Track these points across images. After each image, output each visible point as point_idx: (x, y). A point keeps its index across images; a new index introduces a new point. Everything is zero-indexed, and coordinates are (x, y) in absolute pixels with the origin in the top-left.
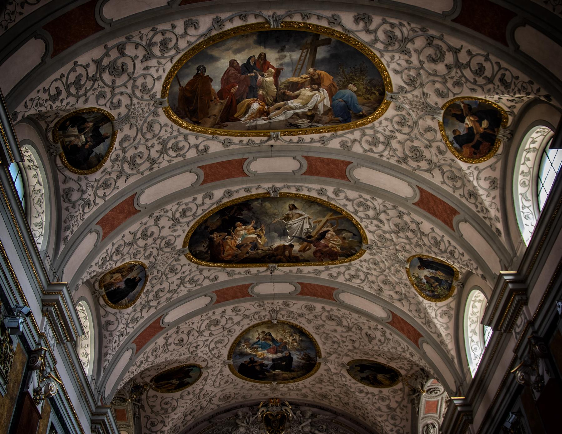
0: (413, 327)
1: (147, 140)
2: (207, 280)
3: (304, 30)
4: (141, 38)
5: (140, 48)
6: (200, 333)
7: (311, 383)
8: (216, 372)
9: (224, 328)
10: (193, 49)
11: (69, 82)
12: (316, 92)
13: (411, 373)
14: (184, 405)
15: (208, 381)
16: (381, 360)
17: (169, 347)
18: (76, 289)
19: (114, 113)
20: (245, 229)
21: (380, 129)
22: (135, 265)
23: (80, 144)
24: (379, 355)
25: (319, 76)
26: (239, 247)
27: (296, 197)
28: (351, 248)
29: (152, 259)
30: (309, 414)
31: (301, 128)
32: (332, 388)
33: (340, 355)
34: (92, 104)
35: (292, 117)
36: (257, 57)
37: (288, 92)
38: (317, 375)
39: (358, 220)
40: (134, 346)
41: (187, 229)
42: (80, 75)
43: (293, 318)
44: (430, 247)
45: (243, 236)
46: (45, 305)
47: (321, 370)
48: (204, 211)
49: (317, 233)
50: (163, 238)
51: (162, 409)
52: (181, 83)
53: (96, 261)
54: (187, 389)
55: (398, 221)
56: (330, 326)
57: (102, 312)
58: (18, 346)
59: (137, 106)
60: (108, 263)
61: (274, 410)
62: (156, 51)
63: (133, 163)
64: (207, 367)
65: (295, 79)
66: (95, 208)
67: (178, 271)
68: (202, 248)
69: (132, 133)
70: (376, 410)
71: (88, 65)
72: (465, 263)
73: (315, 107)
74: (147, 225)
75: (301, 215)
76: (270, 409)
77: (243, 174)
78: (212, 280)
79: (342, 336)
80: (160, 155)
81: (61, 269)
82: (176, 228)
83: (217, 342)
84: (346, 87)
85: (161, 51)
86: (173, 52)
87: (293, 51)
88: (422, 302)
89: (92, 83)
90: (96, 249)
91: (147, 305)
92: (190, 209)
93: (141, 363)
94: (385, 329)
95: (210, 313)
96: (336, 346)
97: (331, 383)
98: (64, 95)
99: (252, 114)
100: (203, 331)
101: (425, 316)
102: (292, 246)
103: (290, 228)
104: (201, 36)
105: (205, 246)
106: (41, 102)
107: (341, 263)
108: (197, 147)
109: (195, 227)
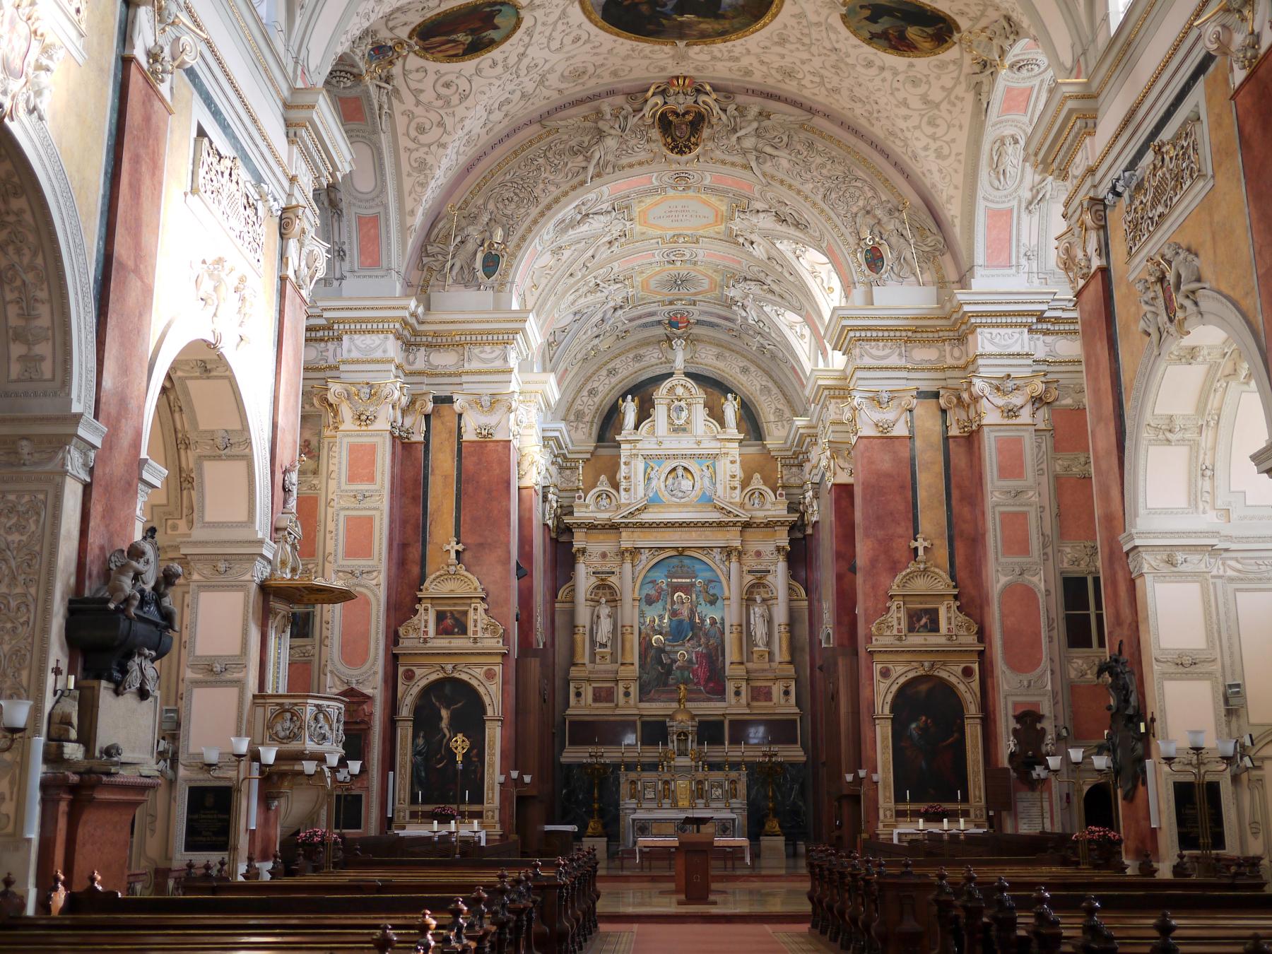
7: (762, 44)
14: (486, 89)
15: (536, 37)
30: (754, 111)
32: (805, 56)
51: (439, 97)
54: (489, 55)
61: (681, 103)
70: (896, 106)
76: (671, 100)
97: (804, 45)
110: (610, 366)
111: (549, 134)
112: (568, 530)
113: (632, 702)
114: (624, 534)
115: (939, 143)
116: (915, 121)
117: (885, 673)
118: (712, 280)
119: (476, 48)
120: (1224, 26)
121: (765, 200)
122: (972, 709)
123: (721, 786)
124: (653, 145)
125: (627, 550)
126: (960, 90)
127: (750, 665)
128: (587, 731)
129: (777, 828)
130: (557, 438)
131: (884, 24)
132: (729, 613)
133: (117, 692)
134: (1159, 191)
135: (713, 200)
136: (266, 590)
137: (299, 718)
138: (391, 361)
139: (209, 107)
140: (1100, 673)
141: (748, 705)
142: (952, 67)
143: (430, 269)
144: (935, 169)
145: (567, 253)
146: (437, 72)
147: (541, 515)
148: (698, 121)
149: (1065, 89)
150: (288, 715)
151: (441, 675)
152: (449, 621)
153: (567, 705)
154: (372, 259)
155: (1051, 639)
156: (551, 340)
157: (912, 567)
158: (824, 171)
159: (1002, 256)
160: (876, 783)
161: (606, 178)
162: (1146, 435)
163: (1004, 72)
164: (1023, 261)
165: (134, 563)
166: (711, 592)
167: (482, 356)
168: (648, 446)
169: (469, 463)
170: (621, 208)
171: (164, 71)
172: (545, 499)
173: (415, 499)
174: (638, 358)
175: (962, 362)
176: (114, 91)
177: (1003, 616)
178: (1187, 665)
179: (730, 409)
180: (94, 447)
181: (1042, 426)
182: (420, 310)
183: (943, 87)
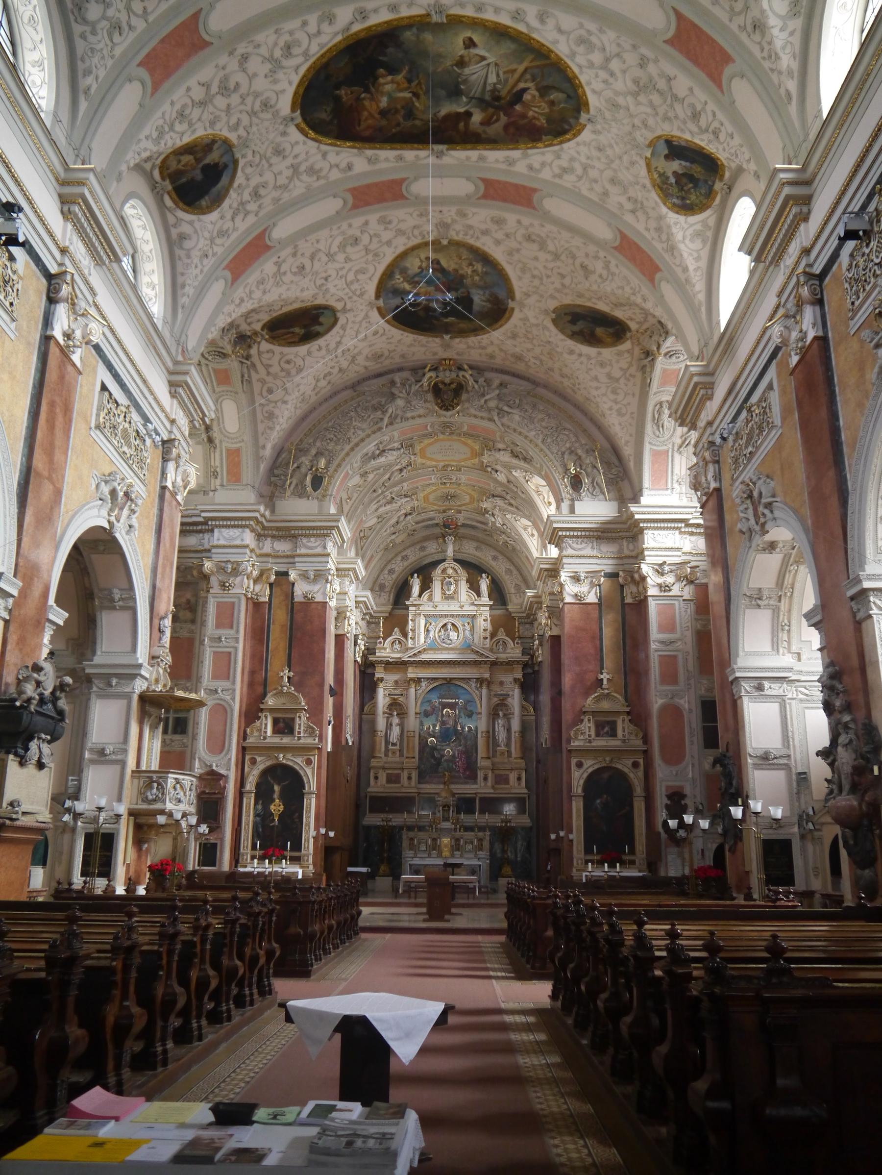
0: (649, 257)
2: (335, 170)
6: (331, 256)
8: (359, 319)
9: (367, 251)
13: (644, 327)
15: (348, 331)
18: (119, 178)
20: (392, 82)
22: (214, 142)
24: (599, 299)
26: (383, 113)
28: (564, 120)
29: (241, 132)
30: (496, 382)
32: (530, 346)
33: (542, 296)
41: (296, 79)
43: (472, 237)
46: (65, 201)
47: (515, 321)
48: (322, 46)
49: (509, 92)
50: (257, 95)
51: (282, 370)
53: (146, 131)
55: (638, 73)
57: (171, 219)
58: (27, 265)
60: (167, 137)
61: (447, 376)
64: (344, 310)
66: (132, 36)
67: (287, 153)
72: (733, 151)
74: (228, 70)
75: (483, 58)
76: (441, 374)
79: (545, 267)
83: (357, 272)
90: (143, 113)
91: (240, 209)
92: (298, 43)
93: (242, 300)
94: (609, 258)
95: (344, 225)
100: (335, 253)
101: (668, 239)
102: (468, 114)
103: (465, 81)
105: (329, 109)
107: (546, 146)
109: (310, 76)
110: (404, 554)
111: (358, 396)
112: (372, 665)
113: (413, 783)
114: (410, 670)
115: (619, 406)
117: (580, 765)
118: (472, 497)
119: (308, 337)
120: (785, 327)
121: (503, 441)
122: (639, 790)
123: (472, 842)
124: (429, 405)
125: (411, 679)
126: (633, 370)
127: (496, 760)
128: (382, 804)
129: (510, 873)
131: (580, 326)
132: (481, 724)
133: (22, 764)
135: (470, 441)
136: (144, 699)
137: (163, 788)
138: (247, 546)
139: (110, 371)
140: (714, 765)
141: (493, 787)
142: (626, 355)
143: (275, 485)
145: (371, 477)
146: (281, 353)
147: (353, 654)
148: (459, 389)
149: (692, 369)
150: (155, 785)
151: (275, 762)
152: (281, 725)
153: (368, 785)
154: (235, 476)
155: (692, 743)
157: (599, 691)
158: (544, 424)
159: (662, 479)
160: (571, 841)
161: (396, 426)
162: (744, 602)
164: (676, 485)
165: (35, 675)
167: (310, 544)
168: (427, 608)
169: (298, 617)
170: (408, 445)
171: (74, 346)
172: (356, 643)
173: (261, 641)
175: (634, 553)
176: (38, 358)
177: (661, 726)
178: (765, 759)
179: (484, 585)
180: (13, 596)
182: (267, 513)
183: (621, 369)
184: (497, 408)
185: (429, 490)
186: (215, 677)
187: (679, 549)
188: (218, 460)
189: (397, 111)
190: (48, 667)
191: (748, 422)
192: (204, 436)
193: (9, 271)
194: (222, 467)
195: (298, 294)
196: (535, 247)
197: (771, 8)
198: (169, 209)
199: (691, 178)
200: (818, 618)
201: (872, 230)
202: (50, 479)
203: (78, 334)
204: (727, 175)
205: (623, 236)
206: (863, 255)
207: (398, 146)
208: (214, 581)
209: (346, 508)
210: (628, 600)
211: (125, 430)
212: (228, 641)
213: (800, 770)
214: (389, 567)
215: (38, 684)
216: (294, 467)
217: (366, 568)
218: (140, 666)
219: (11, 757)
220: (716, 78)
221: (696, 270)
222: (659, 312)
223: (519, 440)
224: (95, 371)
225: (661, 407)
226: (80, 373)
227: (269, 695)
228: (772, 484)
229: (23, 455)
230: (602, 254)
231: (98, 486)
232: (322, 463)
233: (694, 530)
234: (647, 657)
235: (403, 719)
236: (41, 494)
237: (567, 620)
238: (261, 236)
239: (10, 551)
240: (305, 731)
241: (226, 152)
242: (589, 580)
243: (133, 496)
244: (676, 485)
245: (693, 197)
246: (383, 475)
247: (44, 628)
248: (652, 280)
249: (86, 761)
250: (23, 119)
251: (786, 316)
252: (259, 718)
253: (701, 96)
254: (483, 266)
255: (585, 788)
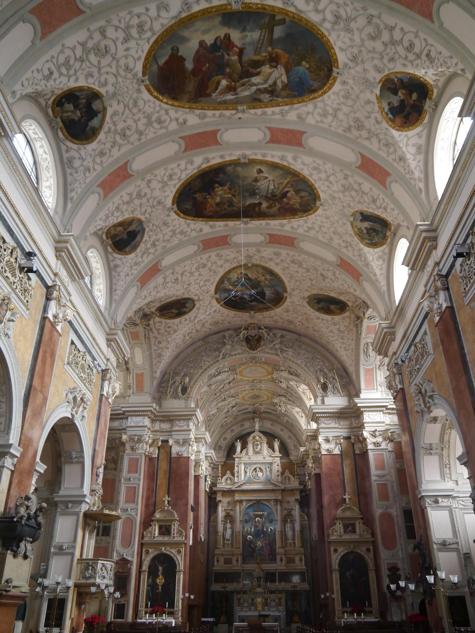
1: (134, 114)
2: (194, 232)
3: (261, 11)
4: (120, 21)
5: (120, 31)
6: (191, 274)
8: (206, 304)
9: (210, 270)
10: (166, 31)
11: (59, 63)
12: (275, 69)
15: (201, 311)
16: (333, 294)
17: (167, 285)
18: (86, 239)
19: (102, 91)
20: (222, 190)
21: (329, 102)
22: (133, 220)
23: (76, 118)
24: (331, 291)
25: (277, 54)
26: (218, 204)
27: (262, 162)
29: (147, 215)
30: (279, 335)
31: (263, 102)
32: (296, 316)
33: (301, 290)
34: (82, 83)
35: (255, 93)
36: (222, 37)
37: (251, 70)
38: (285, 306)
39: (313, 182)
40: (139, 284)
41: (174, 190)
42: (69, 57)
44: (369, 204)
45: (220, 196)
46: (57, 250)
48: (187, 175)
49: (280, 192)
50: (155, 198)
51: (166, 331)
52: (159, 63)
53: (100, 216)
55: (344, 182)
56: (294, 268)
57: (111, 258)
59: (122, 84)
60: (110, 219)
61: (253, 332)
62: (134, 32)
63: (124, 135)
64: (199, 300)
65: (257, 58)
66: (95, 173)
67: (169, 225)
68: (188, 206)
69: (120, 108)
71: (75, 47)
73: (275, 83)
74: (141, 188)
75: (267, 178)
76: (250, 332)
77: (217, 143)
78: (198, 232)
79: (302, 276)
80: (146, 128)
81: (69, 223)
82: (165, 189)
83: (205, 281)
84: (299, 64)
85: (138, 33)
86: (149, 34)
87: (253, 31)
88: (362, 249)
89: (80, 63)
90: (99, 207)
91: (146, 252)
93: (146, 297)
94: (335, 270)
95: (199, 258)
96: (298, 283)
98: (56, 75)
99: (222, 90)
100: (194, 272)
101: (365, 260)
102: (260, 204)
103: (258, 189)
104: (173, 18)
105: (191, 204)
106: (36, 81)
107: (300, 217)
108: (177, 120)
110: (231, 429)
111: (206, 344)
112: (215, 493)
113: (239, 564)
114: (236, 495)
115: (345, 345)
116: (336, 338)
118: (268, 396)
119: (179, 315)
120: (431, 302)
122: (371, 566)
123: (275, 601)
124: (243, 348)
126: (351, 327)
127: (287, 548)
130: (211, 456)
133: (15, 556)
134: (417, 360)
135: (266, 366)
138: (146, 426)
139: (76, 334)
141: (286, 566)
142: (347, 319)
143: (162, 393)
144: (344, 354)
145: (213, 387)
147: (204, 487)
148: (259, 339)
149: (383, 325)
150: (91, 568)
152: (164, 529)
153: (213, 565)
154: (140, 388)
156: (209, 418)
159: (371, 385)
160: (334, 599)
162: (422, 451)
163: (365, 320)
164: (379, 387)
165: (26, 502)
166: (270, 517)
167: (180, 424)
169: (174, 465)
170: (233, 369)
172: (206, 480)
173: (153, 480)
174: (242, 425)
175: (358, 425)
178: (444, 545)
179: (276, 445)
180: (17, 457)
181: (390, 449)
182: (157, 408)
183: (345, 326)
184: (280, 348)
185: (244, 393)
186: (127, 501)
187: (383, 422)
188: (131, 380)
189: (225, 203)
190: (34, 498)
191: (415, 352)
192: (124, 367)
193: (28, 285)
194: (133, 383)
195: (175, 293)
196: (297, 266)
197: (407, 151)
198: (110, 253)
199: (375, 230)
200: (465, 460)
201: (470, 253)
202: (41, 391)
203: (61, 316)
204: (393, 228)
205: (342, 259)
206: (467, 265)
207: (225, 219)
208: (128, 446)
209: (200, 404)
210: (357, 452)
211: (82, 365)
212: (135, 480)
213: (465, 552)
214: (223, 437)
215: (28, 507)
216: (172, 383)
217: (211, 437)
218: (85, 496)
219: (9, 552)
220: (383, 183)
221: (380, 275)
222: (363, 297)
223: (293, 365)
224: (68, 334)
225: (368, 345)
226: (61, 336)
227: (157, 512)
228: (432, 385)
229: (28, 379)
230: (331, 268)
231: (67, 395)
232: (187, 380)
233: (391, 411)
234: (370, 484)
235: (233, 524)
236: (36, 400)
237: (324, 464)
238: (156, 265)
239: (17, 431)
240: (177, 533)
241: (139, 225)
242: (335, 441)
243: (85, 400)
244: (379, 387)
245: (376, 239)
246: (220, 385)
247: (33, 475)
248: (358, 280)
249: (52, 553)
250: (40, 212)
251: (430, 297)
252: (151, 525)
253: (376, 192)
254: (270, 276)
255: (340, 565)
